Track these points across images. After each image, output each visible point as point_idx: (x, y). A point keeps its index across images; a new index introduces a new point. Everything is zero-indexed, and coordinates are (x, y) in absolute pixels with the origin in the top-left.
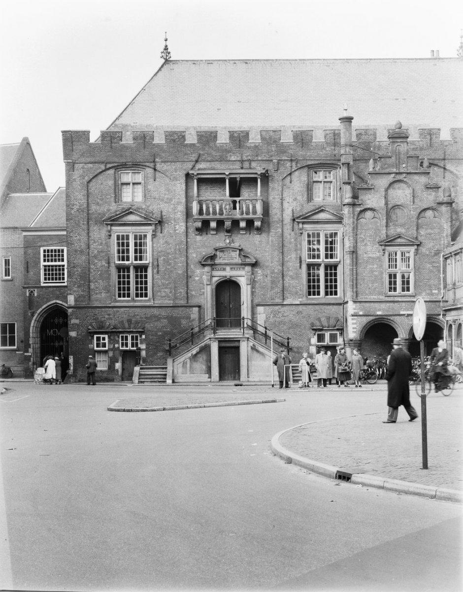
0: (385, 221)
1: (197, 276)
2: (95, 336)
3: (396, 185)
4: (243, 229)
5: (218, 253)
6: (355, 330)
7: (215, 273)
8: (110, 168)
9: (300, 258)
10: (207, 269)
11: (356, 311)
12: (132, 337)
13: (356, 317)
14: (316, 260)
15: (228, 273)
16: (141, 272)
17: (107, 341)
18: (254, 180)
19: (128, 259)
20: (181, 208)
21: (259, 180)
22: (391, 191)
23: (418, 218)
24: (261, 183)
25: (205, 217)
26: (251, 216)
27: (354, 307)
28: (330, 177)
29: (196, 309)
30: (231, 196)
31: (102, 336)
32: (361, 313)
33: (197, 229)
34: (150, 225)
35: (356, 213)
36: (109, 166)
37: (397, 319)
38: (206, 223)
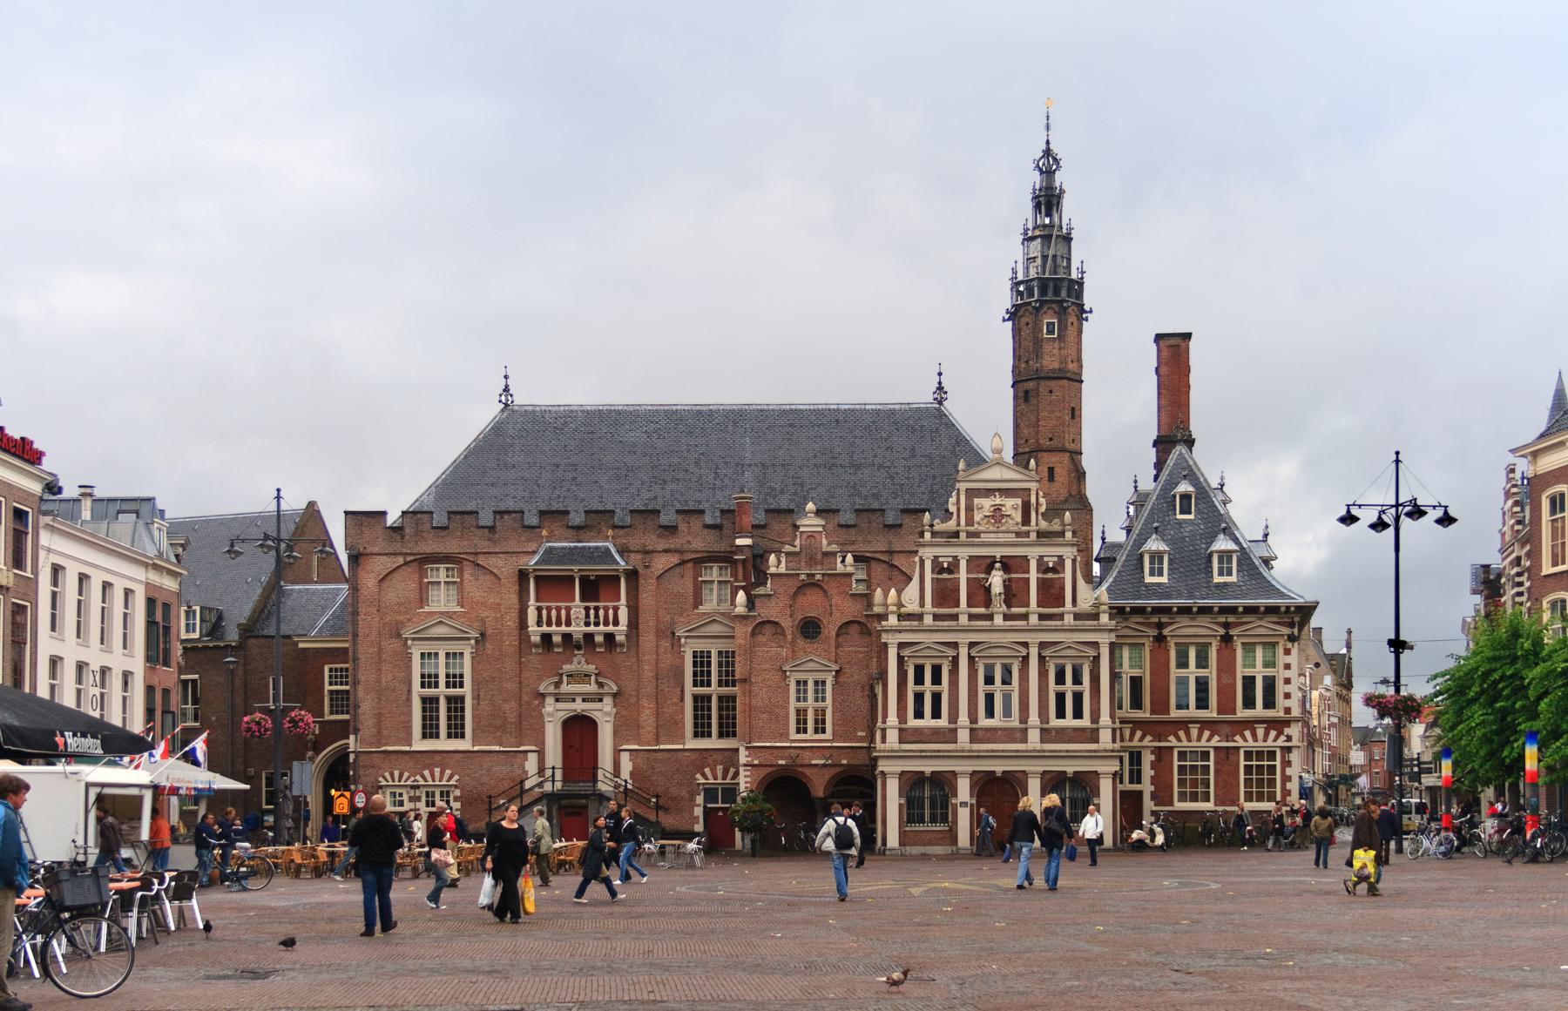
0: (789, 637)
3: (808, 591)
5: (565, 678)
7: (560, 705)
8: (411, 561)
10: (550, 700)
12: (442, 793)
15: (579, 706)
16: (456, 703)
18: (617, 579)
20: (514, 615)
21: (623, 580)
22: (801, 600)
23: (838, 635)
24: (627, 585)
25: (545, 628)
26: (611, 628)
28: (726, 575)
29: (533, 758)
30: (583, 599)
31: (398, 791)
33: (536, 646)
34: (468, 639)
35: (750, 629)
38: (547, 638)
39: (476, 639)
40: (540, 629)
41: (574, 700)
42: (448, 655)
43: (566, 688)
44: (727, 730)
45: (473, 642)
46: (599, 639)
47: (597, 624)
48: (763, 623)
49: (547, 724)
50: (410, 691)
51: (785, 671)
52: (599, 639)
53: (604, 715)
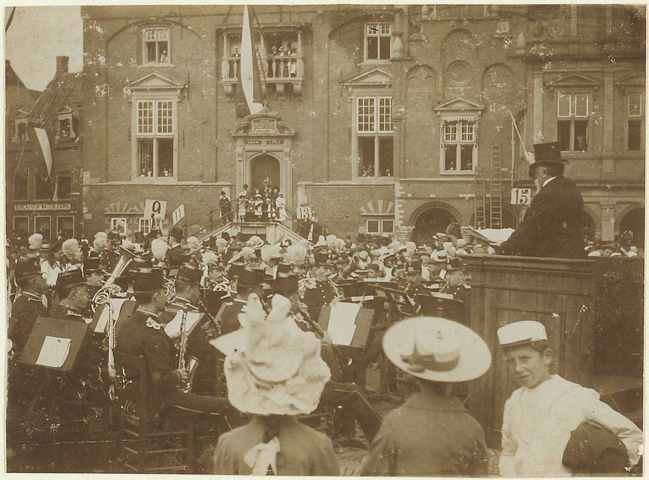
1: (227, 151)
2: (113, 219)
4: (281, 94)
6: (402, 217)
7: (248, 147)
9: (350, 129)
10: (240, 142)
11: (404, 193)
13: (403, 200)
14: (369, 132)
15: (264, 147)
17: (125, 225)
19: (151, 131)
21: (299, 36)
27: (401, 188)
32: (410, 195)
34: (175, 90)
36: (131, 22)
37: (455, 204)
39: (182, 90)
40: (231, 80)
41: (260, 142)
42: (160, 104)
43: (253, 132)
44: (387, 167)
45: (179, 91)
46: (280, 88)
47: (277, 76)
48: (417, 66)
49: (237, 162)
50: (130, 136)
51: (436, 111)
52: (280, 88)
53: (283, 152)
